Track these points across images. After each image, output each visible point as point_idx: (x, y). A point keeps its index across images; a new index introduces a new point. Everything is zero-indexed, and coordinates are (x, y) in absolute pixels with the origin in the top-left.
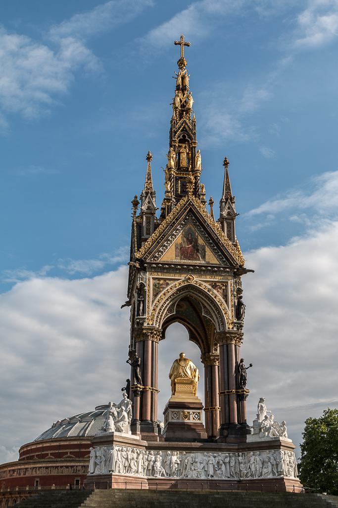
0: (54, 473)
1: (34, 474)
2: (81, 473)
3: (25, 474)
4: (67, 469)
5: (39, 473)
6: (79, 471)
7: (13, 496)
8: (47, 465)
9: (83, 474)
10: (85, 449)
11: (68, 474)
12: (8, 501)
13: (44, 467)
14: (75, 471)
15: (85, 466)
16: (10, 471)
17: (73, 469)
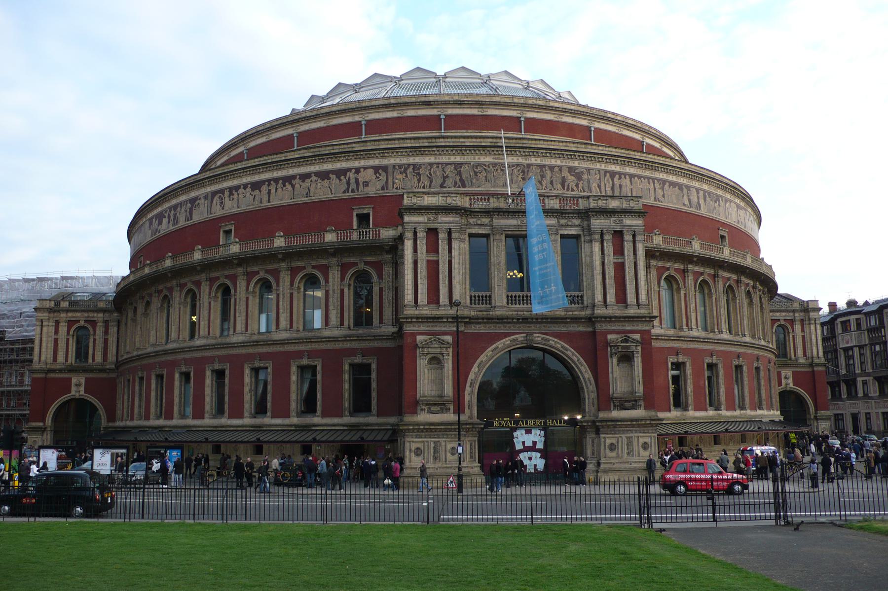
0: (282, 197)
1: (218, 212)
2: (373, 190)
3: (187, 219)
4: (326, 183)
5: (231, 207)
6: (366, 184)
7: (161, 287)
8: (257, 178)
9: (381, 193)
10: (380, 132)
11: (329, 196)
12: (148, 304)
13: (245, 186)
14: (353, 185)
15: (385, 168)
16: (151, 219)
17: (344, 181)
